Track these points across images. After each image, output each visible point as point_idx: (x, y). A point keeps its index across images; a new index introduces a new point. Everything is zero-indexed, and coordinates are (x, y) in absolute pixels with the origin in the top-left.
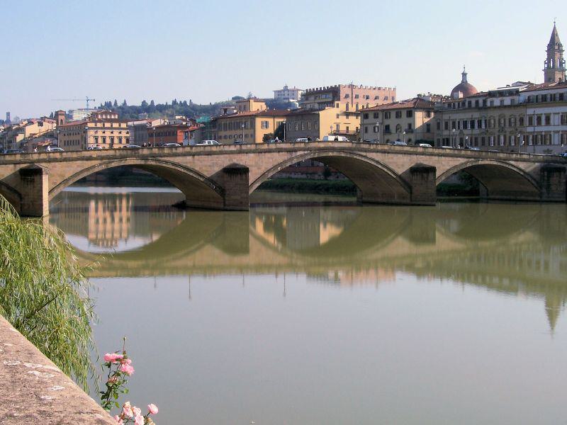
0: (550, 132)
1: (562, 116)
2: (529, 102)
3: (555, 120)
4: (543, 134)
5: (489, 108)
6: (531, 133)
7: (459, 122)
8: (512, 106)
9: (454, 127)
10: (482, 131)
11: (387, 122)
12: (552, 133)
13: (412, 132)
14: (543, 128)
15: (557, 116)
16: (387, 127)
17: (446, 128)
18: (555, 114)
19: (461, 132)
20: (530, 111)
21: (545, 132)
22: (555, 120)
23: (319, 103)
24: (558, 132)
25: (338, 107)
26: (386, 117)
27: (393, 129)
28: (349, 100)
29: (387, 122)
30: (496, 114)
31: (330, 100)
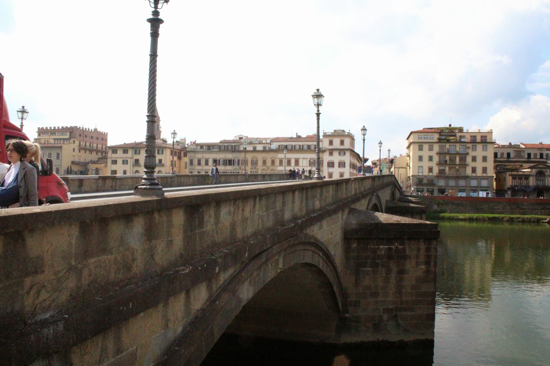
1: (310, 161)
2: (279, 150)
11: (136, 157)
15: (305, 160)
17: (199, 164)
18: (303, 158)
20: (281, 156)
23: (55, 139)
25: (74, 143)
26: (136, 153)
28: (81, 138)
29: (136, 157)
30: (249, 157)
31: (68, 137)
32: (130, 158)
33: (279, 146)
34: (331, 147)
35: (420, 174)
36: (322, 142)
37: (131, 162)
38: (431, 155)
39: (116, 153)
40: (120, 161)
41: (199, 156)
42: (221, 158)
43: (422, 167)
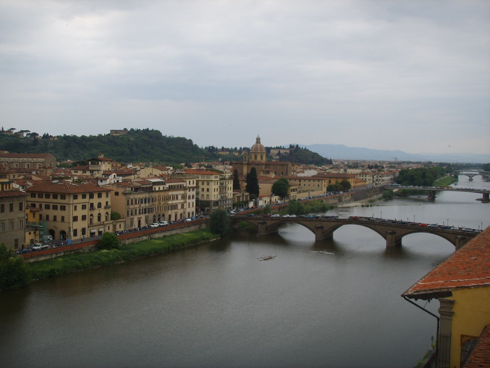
0: (177, 203)
3: (180, 197)
4: (175, 204)
5: (158, 191)
6: (171, 204)
7: (139, 199)
8: (164, 191)
9: (136, 203)
10: (150, 204)
11: (92, 201)
12: (178, 204)
13: (109, 208)
14: (175, 202)
16: (92, 205)
17: (132, 204)
18: (179, 194)
19: (140, 206)
20: (170, 193)
21: (175, 203)
22: (180, 197)
24: (180, 203)
27: (96, 205)
29: (92, 201)
32: (87, 203)
33: (169, 186)
34: (190, 186)
35: (208, 199)
36: (185, 183)
37: (88, 206)
38: (208, 186)
39: (65, 199)
40: (79, 207)
41: (132, 197)
42: (144, 197)
43: (208, 195)
